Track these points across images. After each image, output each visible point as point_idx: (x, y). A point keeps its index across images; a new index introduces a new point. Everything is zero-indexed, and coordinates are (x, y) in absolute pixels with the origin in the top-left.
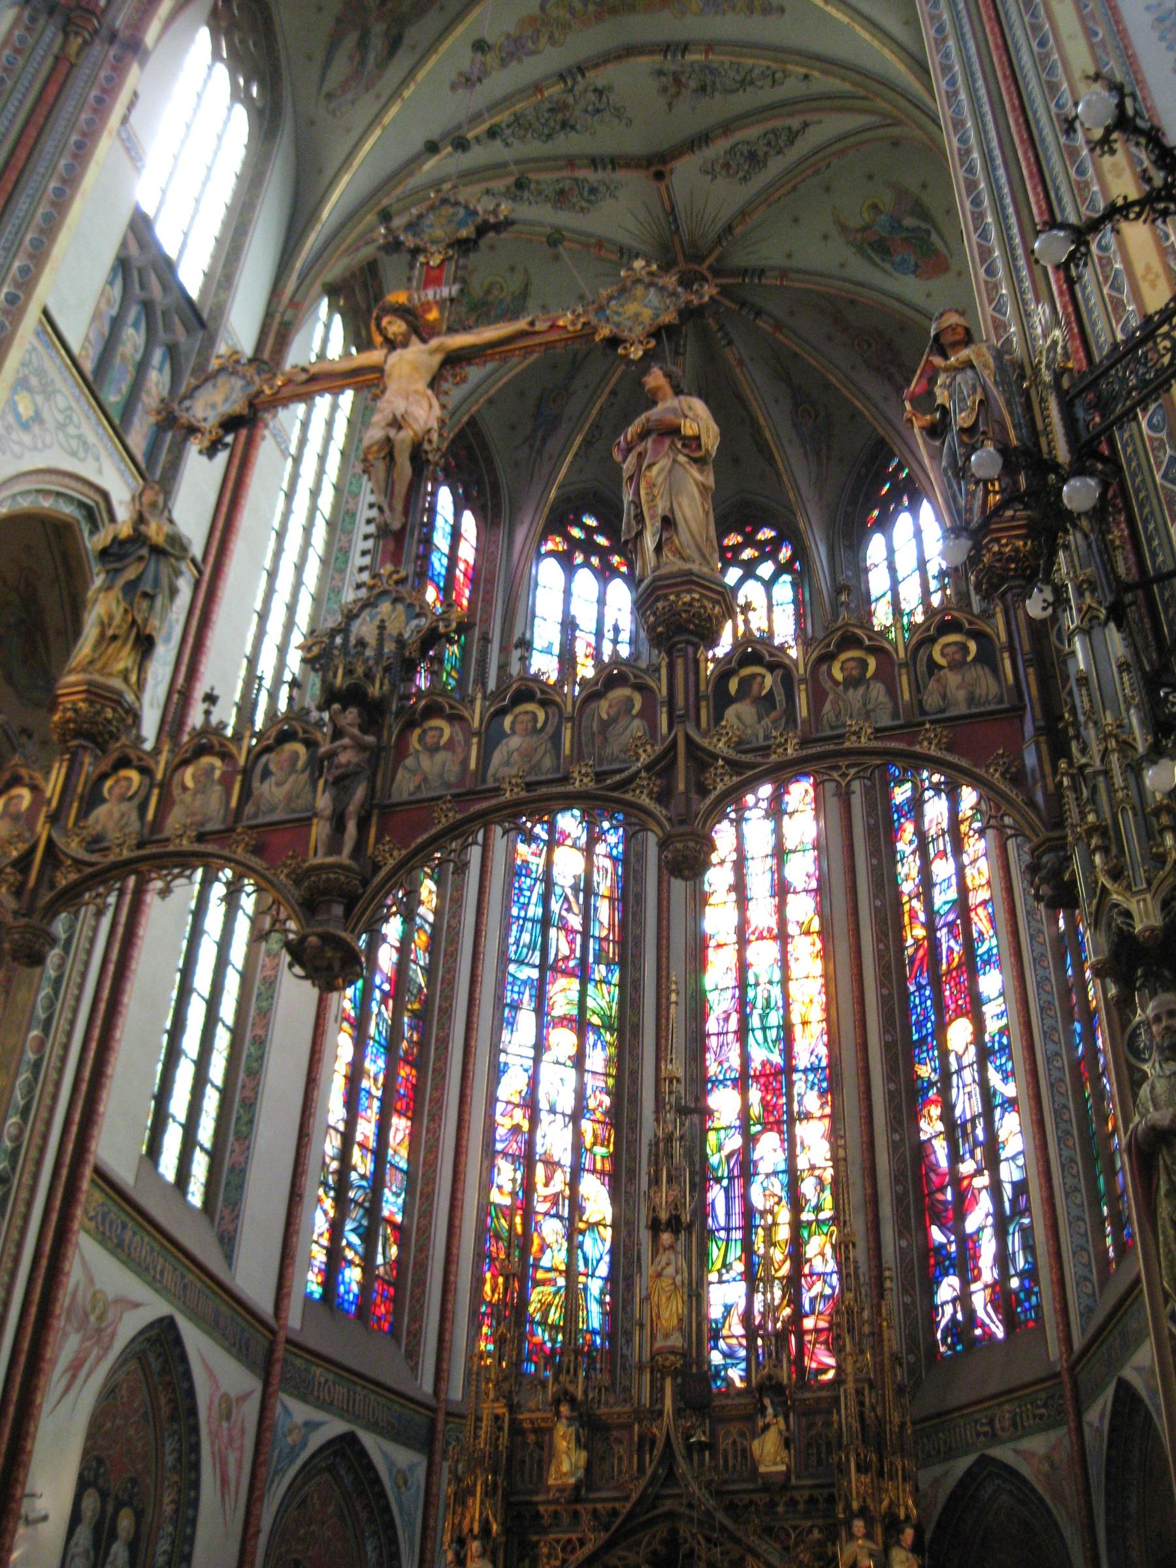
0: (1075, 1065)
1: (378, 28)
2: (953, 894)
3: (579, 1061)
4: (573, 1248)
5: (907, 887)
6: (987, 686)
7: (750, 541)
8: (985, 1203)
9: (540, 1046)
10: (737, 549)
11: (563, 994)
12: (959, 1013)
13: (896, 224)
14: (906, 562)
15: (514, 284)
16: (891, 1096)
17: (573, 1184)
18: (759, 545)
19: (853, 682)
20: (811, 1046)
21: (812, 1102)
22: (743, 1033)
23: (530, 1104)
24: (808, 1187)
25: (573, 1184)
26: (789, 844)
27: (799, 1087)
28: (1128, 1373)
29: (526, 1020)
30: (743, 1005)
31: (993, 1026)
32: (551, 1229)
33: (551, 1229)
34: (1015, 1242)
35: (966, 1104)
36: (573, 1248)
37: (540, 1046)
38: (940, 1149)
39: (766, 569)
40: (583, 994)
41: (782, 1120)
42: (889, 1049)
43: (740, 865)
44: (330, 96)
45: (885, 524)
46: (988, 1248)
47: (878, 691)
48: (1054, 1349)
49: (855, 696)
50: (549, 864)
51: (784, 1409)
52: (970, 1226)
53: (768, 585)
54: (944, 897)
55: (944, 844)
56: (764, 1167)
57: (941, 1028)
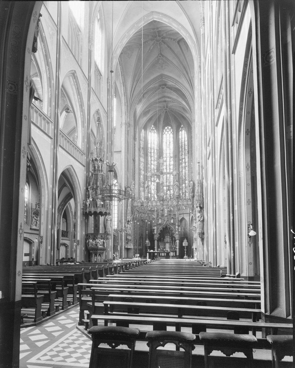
2: (184, 173)
5: (180, 171)
9: (151, 184)
10: (167, 129)
14: (183, 137)
18: (169, 129)
20: (172, 183)
21: (172, 188)
22: (166, 182)
24: (171, 195)
26: (171, 164)
27: (171, 187)
35: (184, 191)
37: (151, 184)
38: (181, 194)
39: (170, 132)
40: (154, 179)
41: (169, 190)
43: (166, 166)
45: (181, 131)
50: (151, 167)
54: (184, 173)
55: (184, 168)
56: (168, 194)
57: (182, 184)
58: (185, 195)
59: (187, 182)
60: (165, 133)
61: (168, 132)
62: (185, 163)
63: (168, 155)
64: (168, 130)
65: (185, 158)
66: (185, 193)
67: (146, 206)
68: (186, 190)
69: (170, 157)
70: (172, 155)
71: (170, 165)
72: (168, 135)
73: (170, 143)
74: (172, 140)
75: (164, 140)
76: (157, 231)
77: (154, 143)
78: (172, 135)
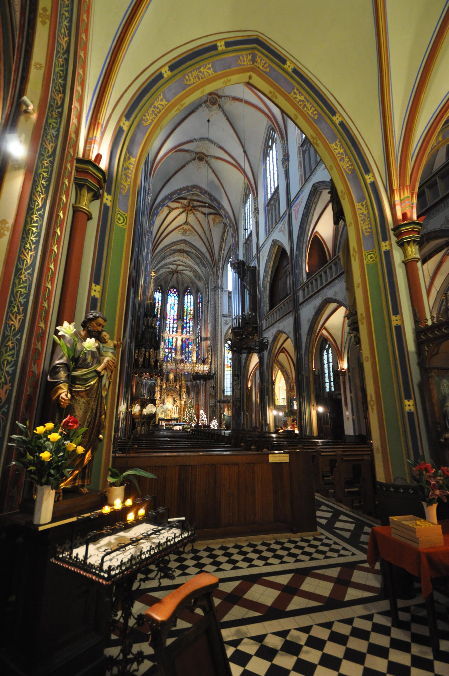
7: (173, 291)
21: (174, 352)
30: (169, 342)
39: (175, 295)
41: (171, 353)
43: (169, 328)
45: (187, 295)
57: (185, 349)
59: (190, 346)
60: (170, 295)
61: (173, 294)
62: (190, 327)
63: (172, 317)
64: (173, 292)
65: (189, 323)
69: (174, 319)
70: (175, 317)
71: (173, 327)
72: (173, 297)
73: (174, 305)
74: (176, 302)
75: (169, 301)
77: (158, 302)
78: (177, 298)
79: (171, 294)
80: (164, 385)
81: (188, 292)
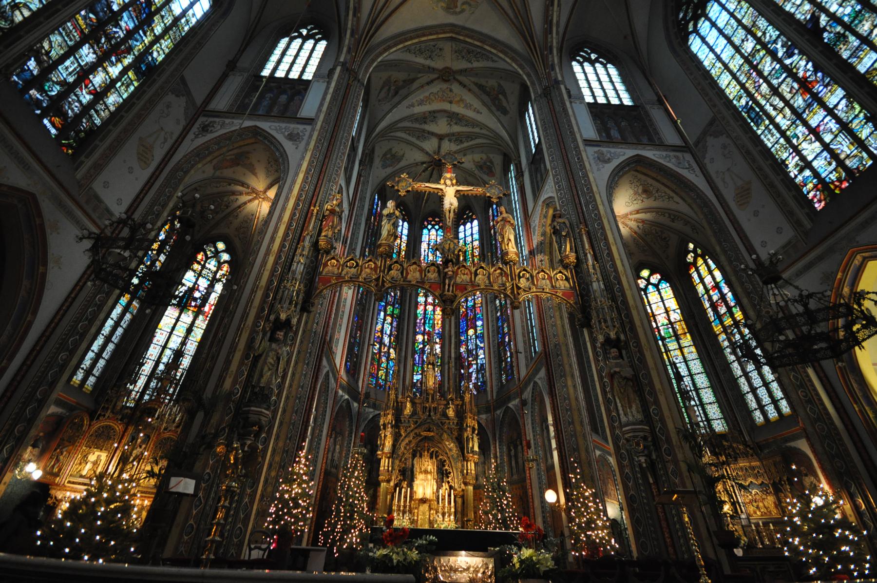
0: (498, 343)
1: (393, 88)
3: (391, 324)
4: (388, 363)
6: (567, 285)
7: (434, 220)
8: (475, 366)
9: (385, 320)
11: (390, 309)
12: (471, 328)
13: (485, 163)
14: (468, 232)
15: (401, 153)
16: (456, 342)
17: (389, 350)
19: (544, 279)
20: (438, 328)
21: (438, 340)
23: (382, 331)
25: (389, 350)
28: (510, 405)
29: (382, 314)
30: (425, 318)
31: (479, 332)
32: (384, 359)
33: (384, 359)
34: (480, 376)
36: (388, 363)
37: (385, 320)
39: (437, 227)
41: (430, 342)
42: (456, 332)
44: (379, 101)
45: (464, 224)
46: (474, 375)
47: (548, 281)
48: (489, 398)
49: (544, 281)
51: (453, 404)
52: (471, 370)
53: (437, 231)
58: (477, 355)
59: (479, 323)
60: (426, 227)
66: (476, 349)
67: (377, 279)
68: (478, 342)
76: (394, 446)
79: (430, 227)
80: (408, 405)
81: (464, 219)
